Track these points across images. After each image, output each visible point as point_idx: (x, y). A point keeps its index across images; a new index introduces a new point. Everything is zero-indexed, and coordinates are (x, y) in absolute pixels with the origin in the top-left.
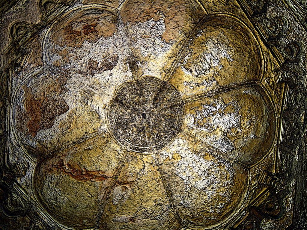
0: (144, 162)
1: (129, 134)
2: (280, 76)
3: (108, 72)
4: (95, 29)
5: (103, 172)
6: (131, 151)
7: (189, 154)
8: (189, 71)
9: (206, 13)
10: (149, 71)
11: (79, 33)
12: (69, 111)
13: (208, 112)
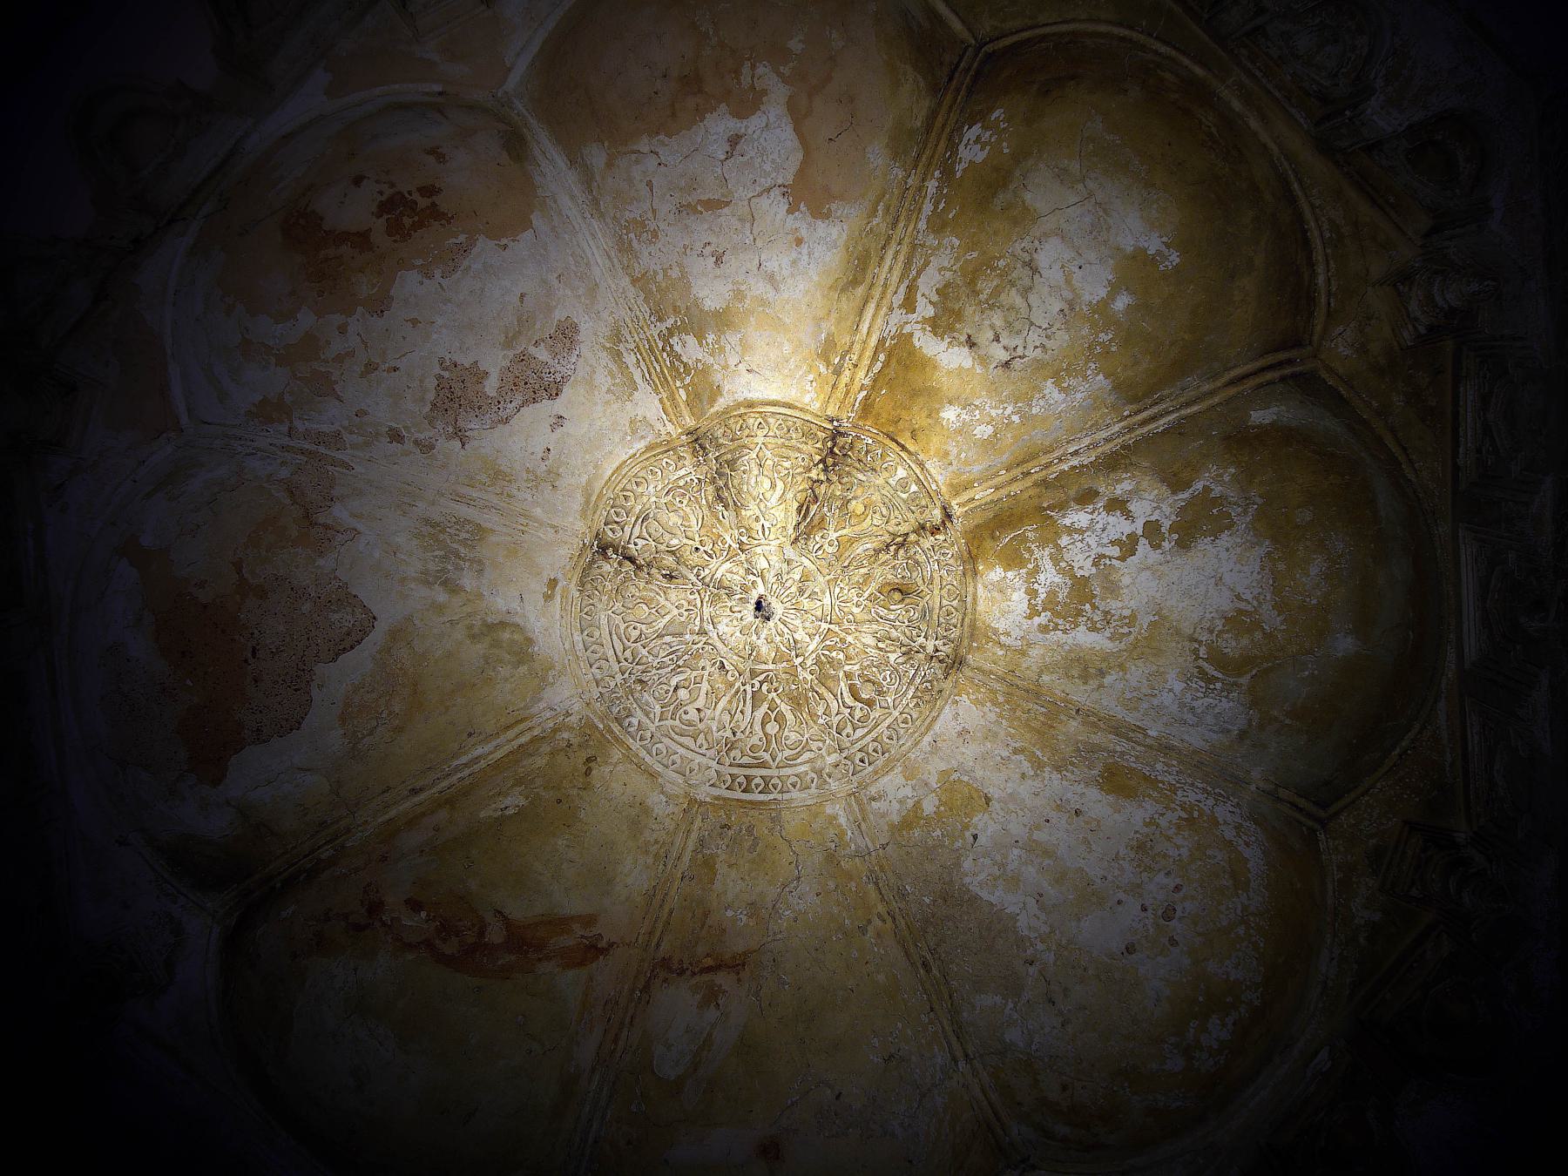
0: (794, 843)
1: (698, 710)
2: (1413, 306)
3: (546, 408)
4: (434, 204)
5: (589, 920)
6: (717, 798)
7: (1023, 776)
8: (960, 344)
9: (966, 35)
10: (750, 376)
11: (362, 239)
12: (377, 636)
13: (1094, 546)
